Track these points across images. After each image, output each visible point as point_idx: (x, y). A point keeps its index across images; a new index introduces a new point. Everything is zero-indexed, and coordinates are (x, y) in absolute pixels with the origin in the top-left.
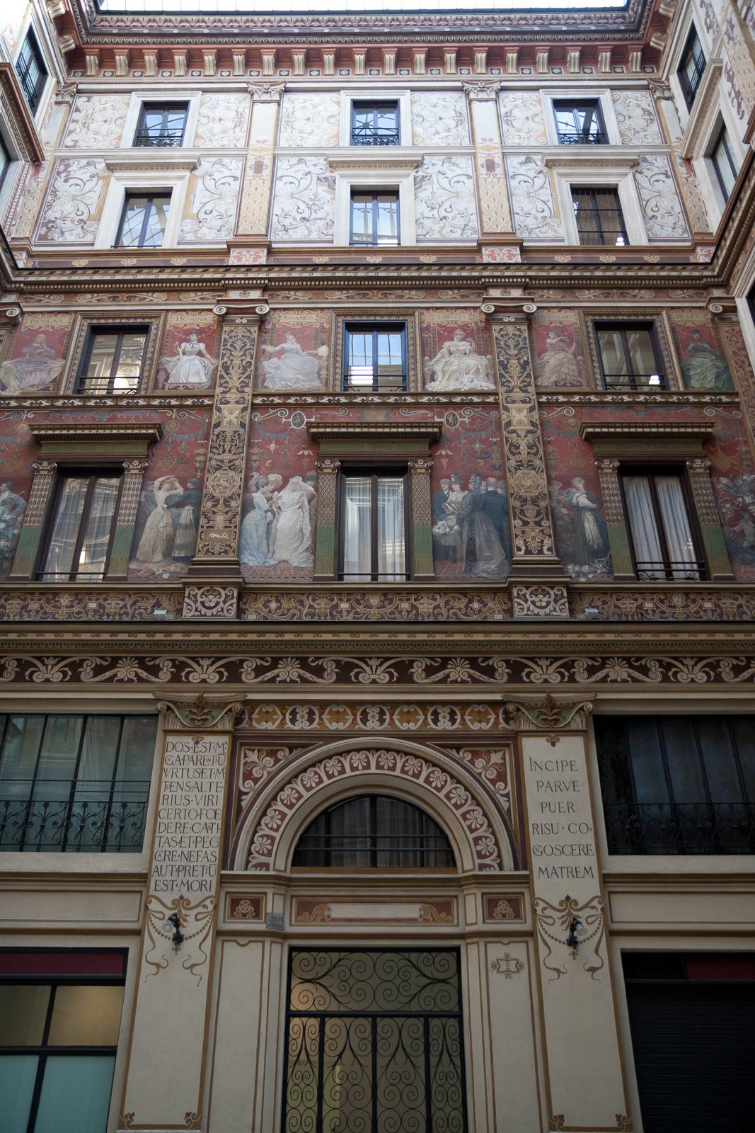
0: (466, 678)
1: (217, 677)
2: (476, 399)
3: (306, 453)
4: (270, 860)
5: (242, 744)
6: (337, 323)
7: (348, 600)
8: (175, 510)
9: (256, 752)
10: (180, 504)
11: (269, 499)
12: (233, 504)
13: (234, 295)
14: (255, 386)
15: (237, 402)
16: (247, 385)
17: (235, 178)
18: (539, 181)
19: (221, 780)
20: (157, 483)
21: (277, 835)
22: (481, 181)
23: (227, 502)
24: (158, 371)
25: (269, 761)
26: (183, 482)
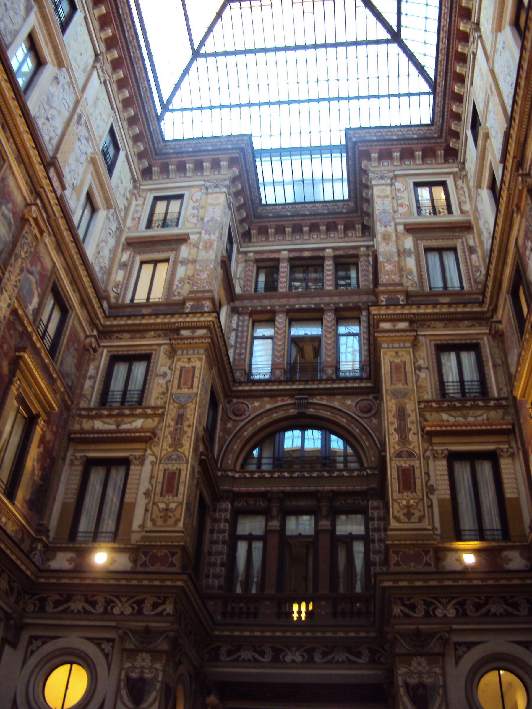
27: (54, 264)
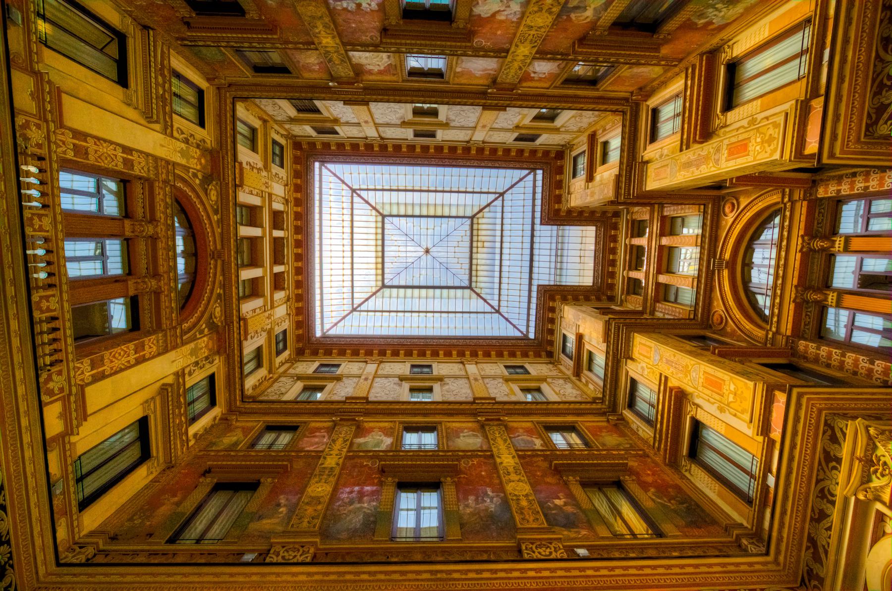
8: (581, 5)
10: (576, 8)
11: (509, 7)
12: (536, 9)
14: (503, 63)
18: (340, 116)
20: (588, 20)
23: (541, 10)
24: (564, 68)
26: (569, 19)
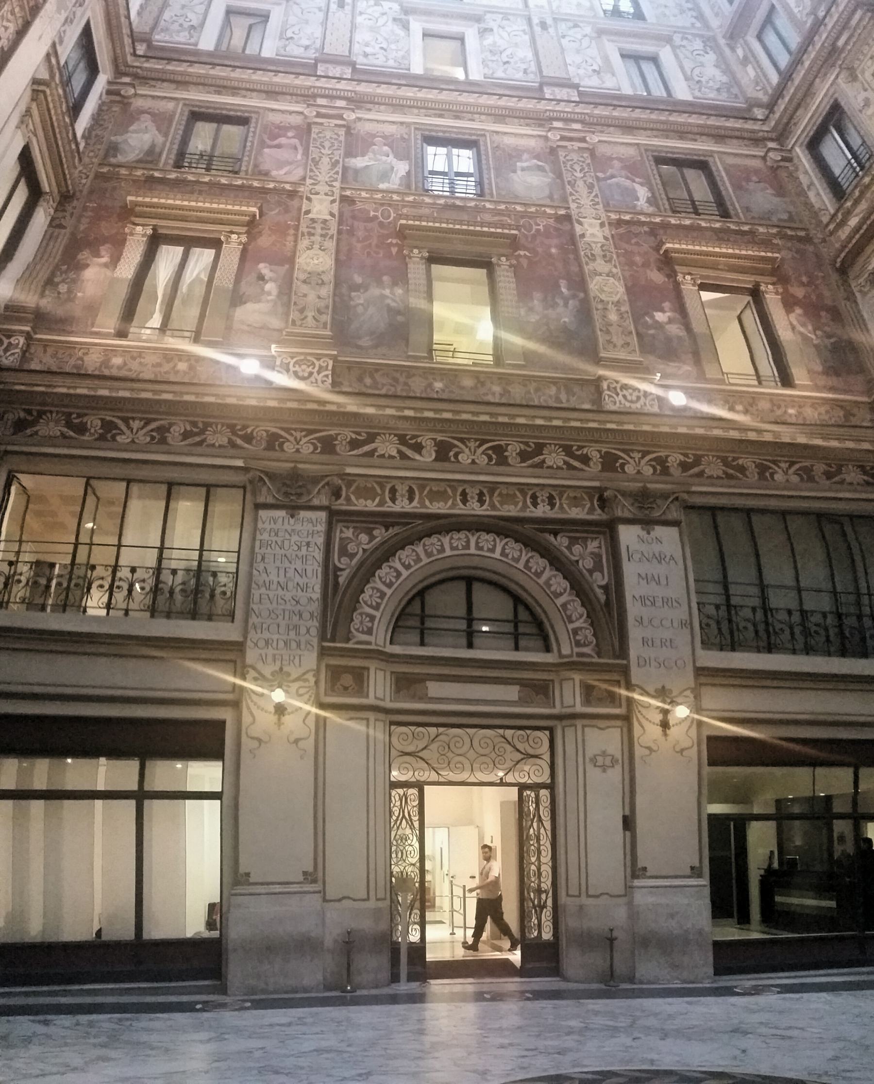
0: (561, 464)
1: (311, 448)
2: (549, 211)
3: (394, 241)
4: (372, 639)
5: (338, 521)
6: (415, 135)
7: (442, 380)
9: (351, 530)
13: (321, 101)
15: (326, 194)
16: (336, 180)
17: (320, 9)
19: (319, 556)
21: (378, 614)
22: (537, 38)
25: (364, 538)
27: (638, 144)
